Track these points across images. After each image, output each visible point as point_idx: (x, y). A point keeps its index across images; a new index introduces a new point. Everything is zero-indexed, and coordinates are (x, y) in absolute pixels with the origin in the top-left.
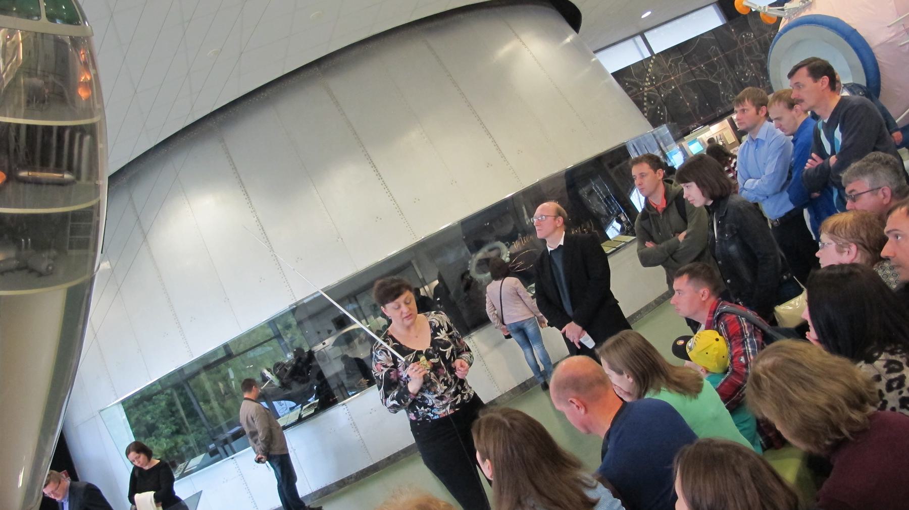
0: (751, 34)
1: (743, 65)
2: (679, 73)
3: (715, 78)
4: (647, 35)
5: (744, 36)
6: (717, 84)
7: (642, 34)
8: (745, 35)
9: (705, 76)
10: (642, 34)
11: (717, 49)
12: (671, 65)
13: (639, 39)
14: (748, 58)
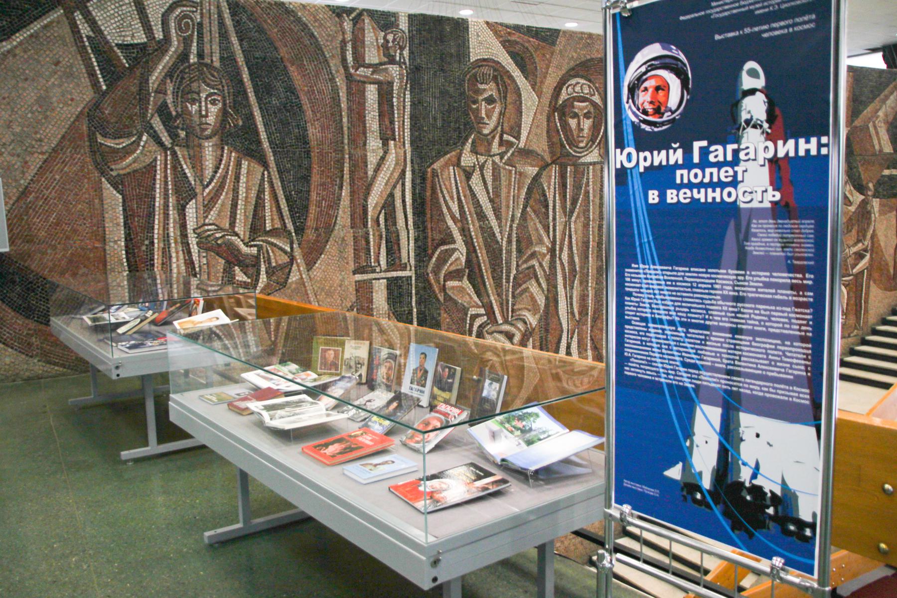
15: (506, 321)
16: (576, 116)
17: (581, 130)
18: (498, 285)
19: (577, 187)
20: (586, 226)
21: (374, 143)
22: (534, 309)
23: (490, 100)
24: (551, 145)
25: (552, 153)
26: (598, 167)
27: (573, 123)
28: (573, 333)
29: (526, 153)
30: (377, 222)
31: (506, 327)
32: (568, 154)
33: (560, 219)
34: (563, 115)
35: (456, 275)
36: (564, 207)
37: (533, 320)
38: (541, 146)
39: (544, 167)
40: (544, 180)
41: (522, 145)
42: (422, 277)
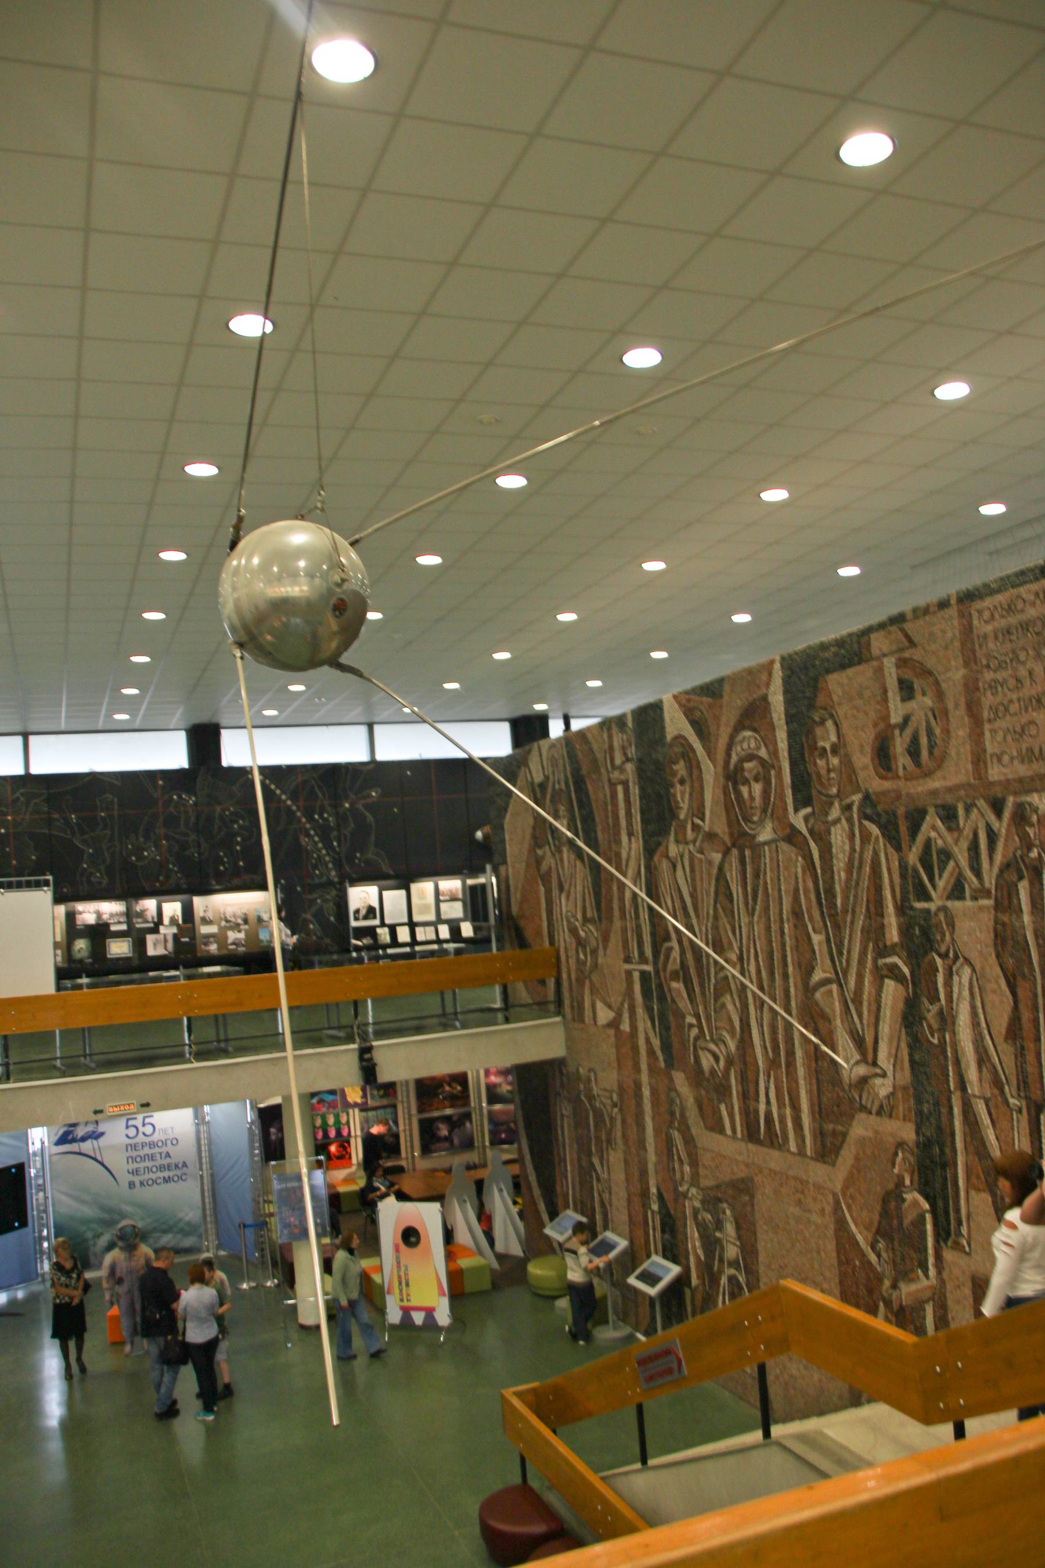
0: (190, 799)
1: (147, 838)
2: (25, 814)
3: (85, 842)
4: (32, 739)
5: (175, 797)
6: (83, 851)
7: (25, 736)
8: (180, 797)
9: (69, 832)
10: (25, 736)
11: (116, 800)
12: (18, 799)
13: (19, 740)
14: (161, 831)
15: (712, 1040)
16: (746, 782)
17: (752, 798)
18: (703, 994)
19: (757, 875)
20: (768, 929)
21: (624, 839)
22: (732, 1032)
23: (682, 782)
24: (730, 825)
25: (731, 835)
26: (774, 846)
27: (744, 790)
28: (769, 1076)
29: (711, 836)
30: (630, 913)
31: (712, 1047)
32: (745, 834)
33: (745, 920)
34: (735, 784)
35: (675, 976)
36: (746, 904)
37: (732, 1045)
38: (721, 828)
39: (726, 853)
40: (726, 865)
41: (707, 829)
42: (657, 972)
